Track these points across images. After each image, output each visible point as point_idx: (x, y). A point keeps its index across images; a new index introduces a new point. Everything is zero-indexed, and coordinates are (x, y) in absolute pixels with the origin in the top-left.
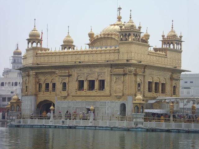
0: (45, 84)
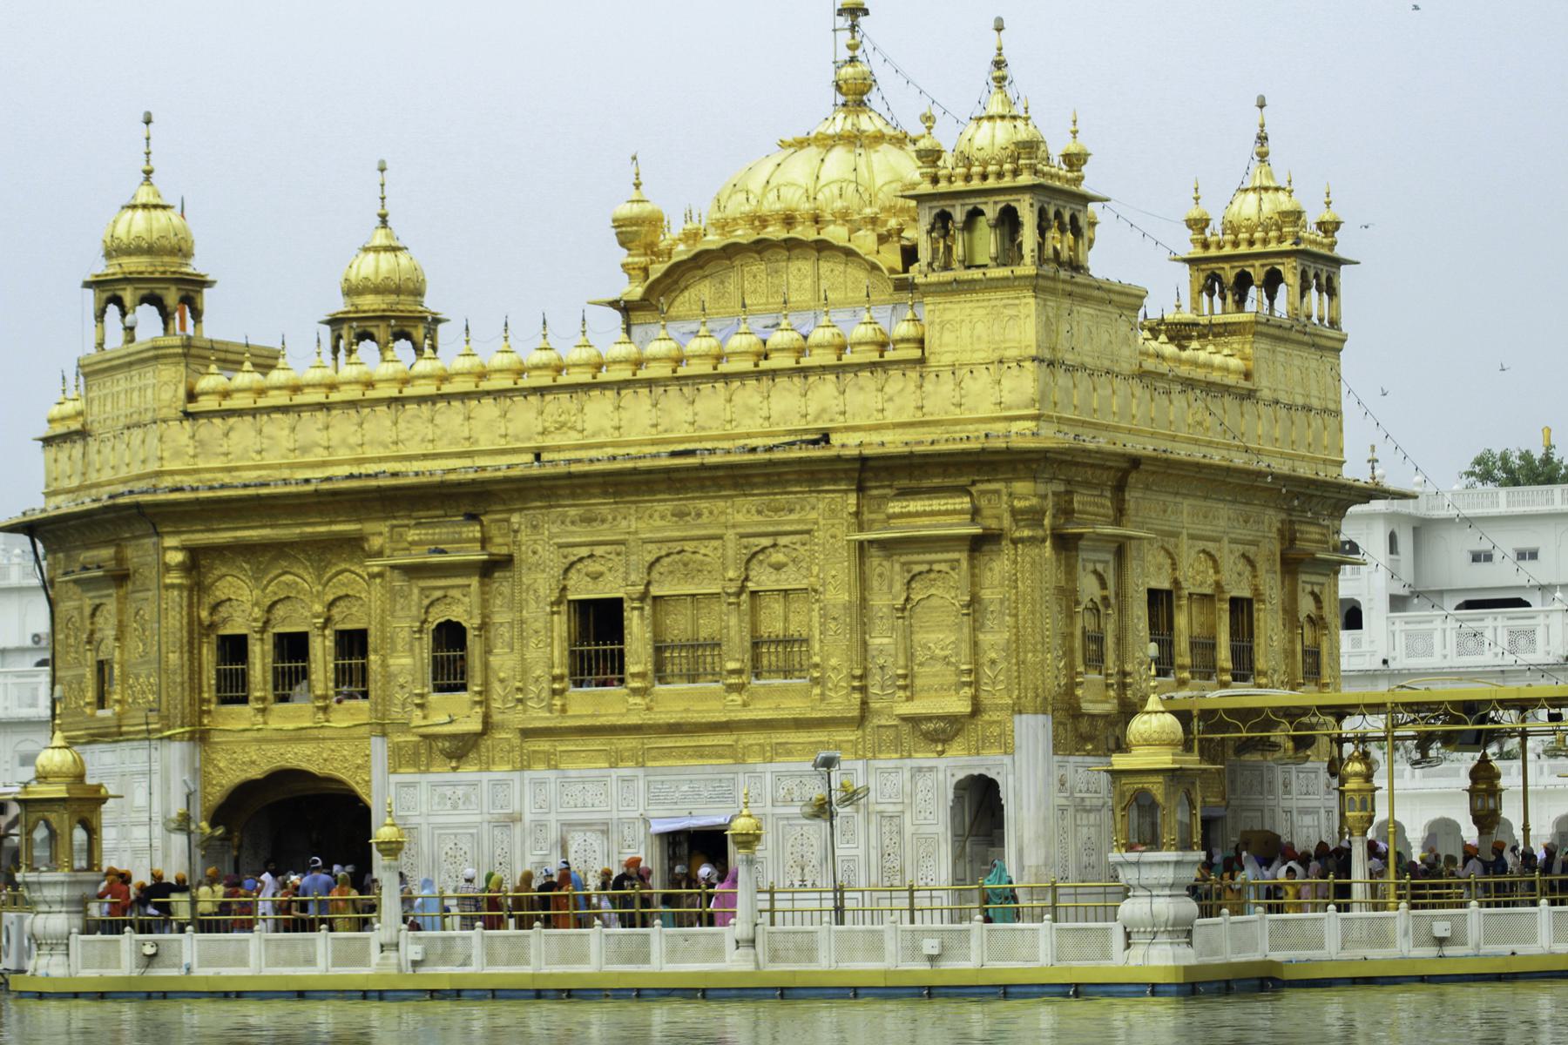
0: (268, 637)
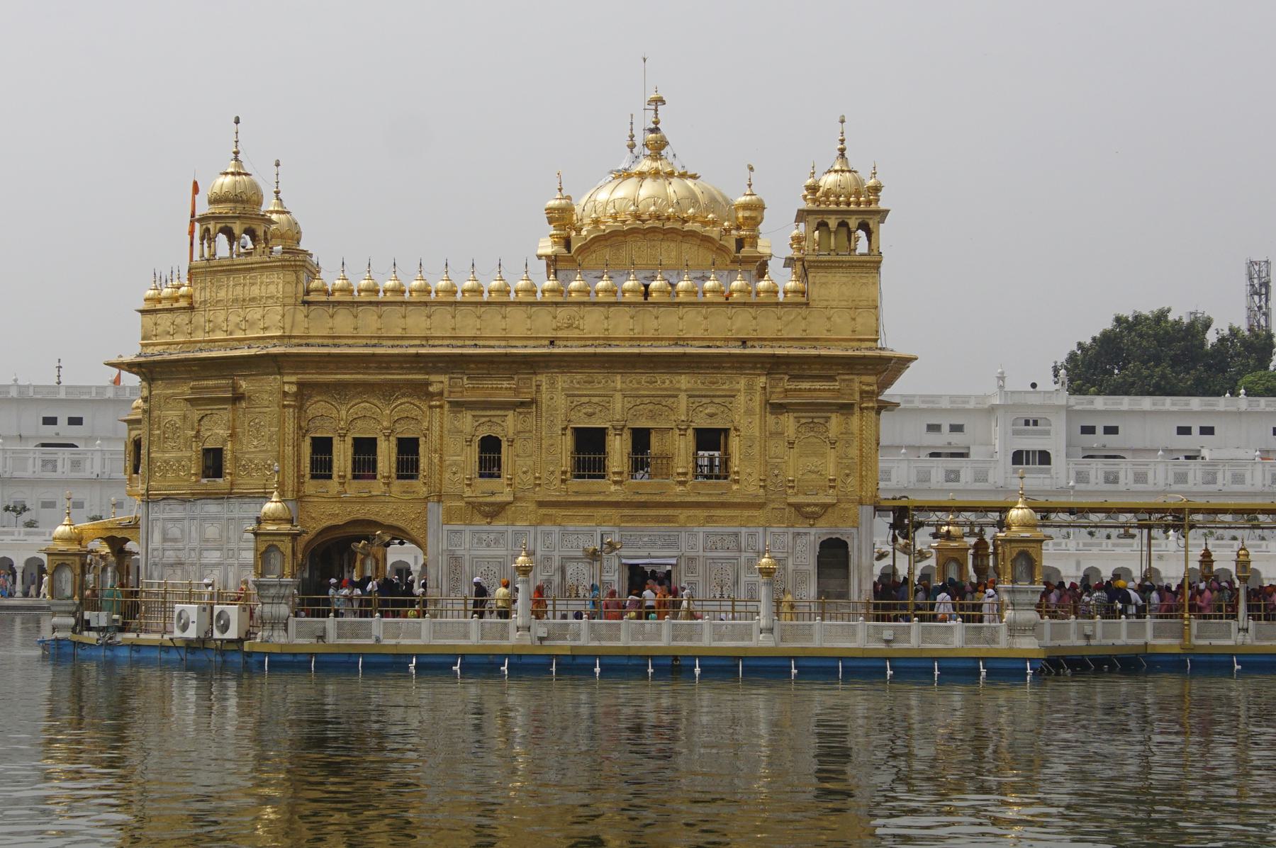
0: (349, 441)
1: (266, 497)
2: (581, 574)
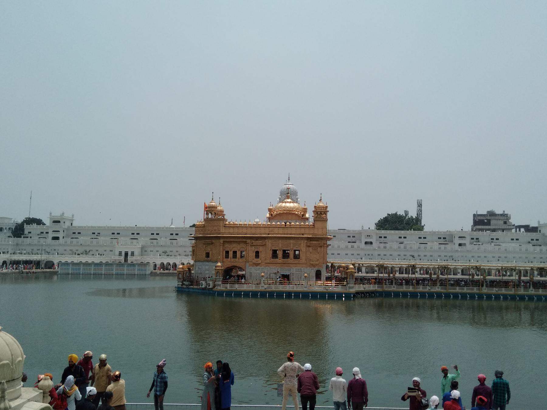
1: (217, 262)
2: (273, 276)
